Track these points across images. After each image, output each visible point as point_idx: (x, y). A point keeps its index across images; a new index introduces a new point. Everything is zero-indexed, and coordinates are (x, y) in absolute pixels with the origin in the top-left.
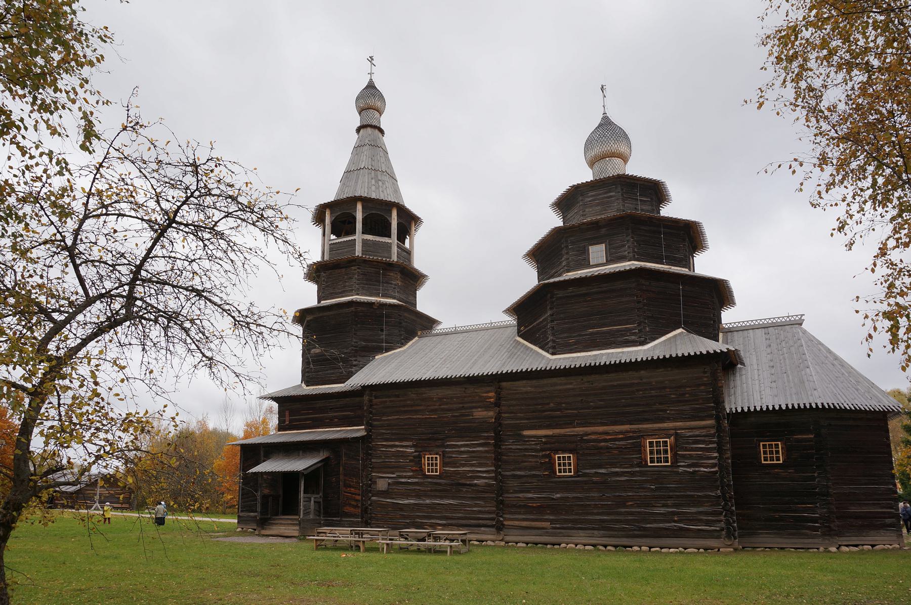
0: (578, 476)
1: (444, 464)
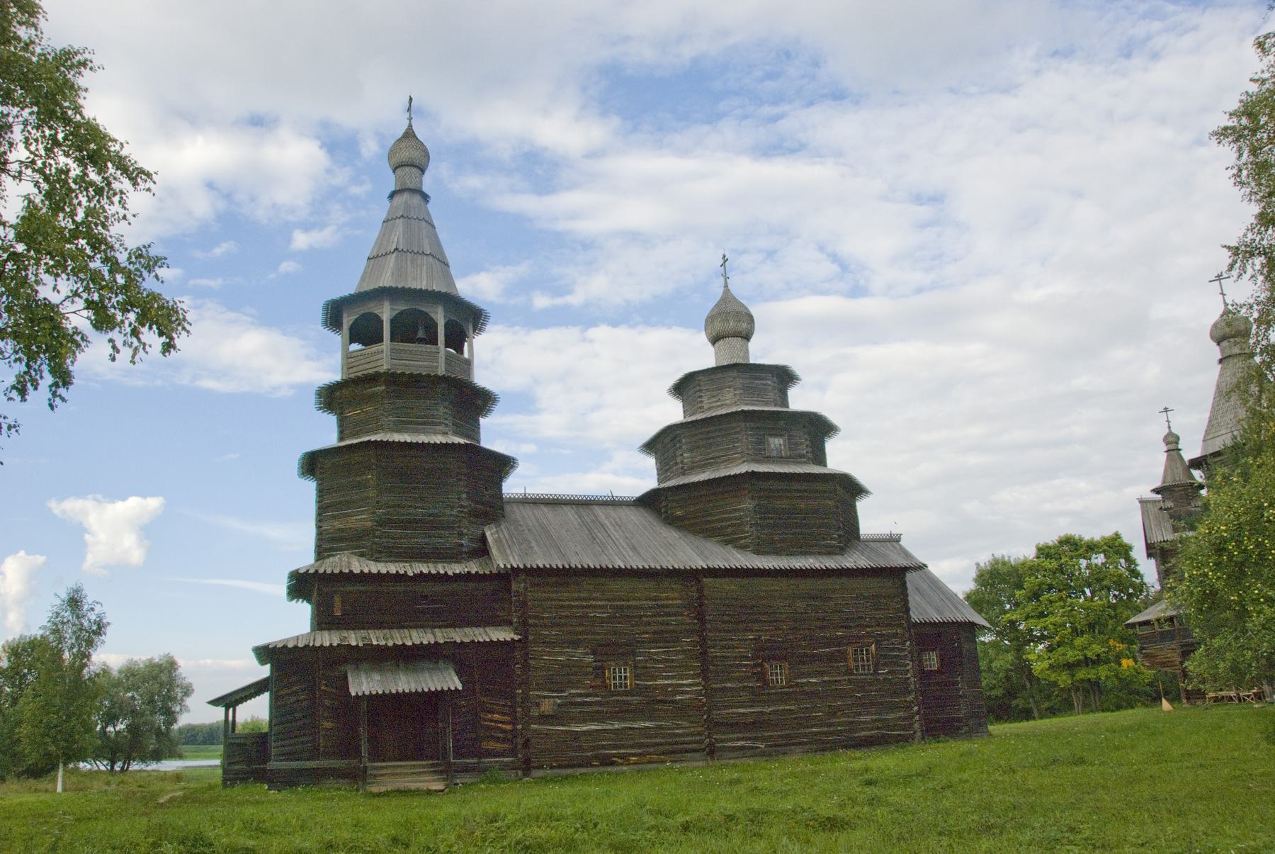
0: (791, 687)
1: (637, 677)
